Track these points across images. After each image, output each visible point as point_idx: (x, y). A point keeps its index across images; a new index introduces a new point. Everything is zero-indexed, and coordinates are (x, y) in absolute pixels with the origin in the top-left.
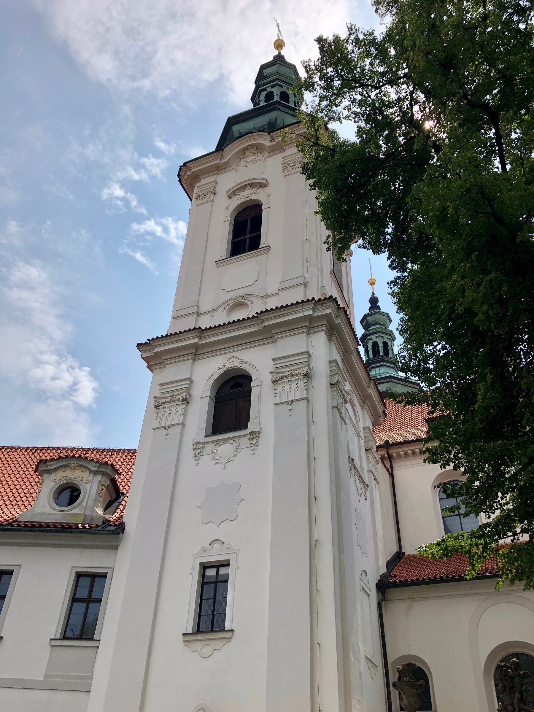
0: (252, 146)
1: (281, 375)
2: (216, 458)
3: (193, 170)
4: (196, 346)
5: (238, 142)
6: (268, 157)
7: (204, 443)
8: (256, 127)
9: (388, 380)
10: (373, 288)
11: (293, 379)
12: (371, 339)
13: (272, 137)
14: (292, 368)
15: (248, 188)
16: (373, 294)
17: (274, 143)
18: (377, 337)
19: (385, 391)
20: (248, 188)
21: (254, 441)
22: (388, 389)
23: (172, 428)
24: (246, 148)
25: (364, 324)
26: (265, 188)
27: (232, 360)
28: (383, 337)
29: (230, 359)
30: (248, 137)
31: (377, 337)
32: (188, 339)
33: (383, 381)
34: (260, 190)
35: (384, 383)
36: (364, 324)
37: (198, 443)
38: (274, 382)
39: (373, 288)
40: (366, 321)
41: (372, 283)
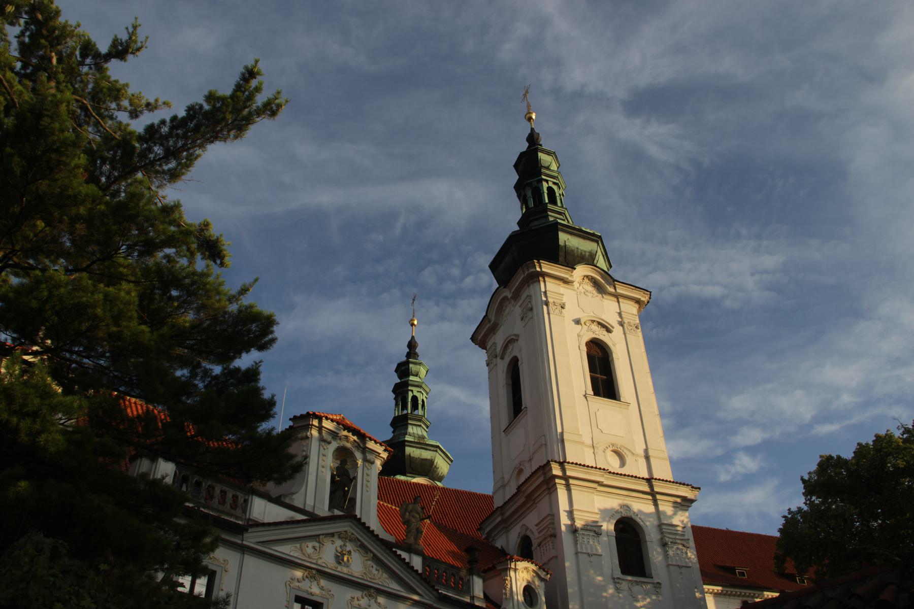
1: (671, 540)
2: (634, 596)
5: (584, 267)
8: (579, 248)
9: (435, 449)
12: (412, 391)
16: (413, 337)
18: (418, 391)
19: (429, 460)
21: (658, 590)
22: (433, 458)
23: (594, 556)
25: (403, 368)
28: (423, 394)
31: (418, 391)
32: (595, 475)
33: (430, 448)
35: (430, 450)
36: (403, 368)
37: (619, 578)
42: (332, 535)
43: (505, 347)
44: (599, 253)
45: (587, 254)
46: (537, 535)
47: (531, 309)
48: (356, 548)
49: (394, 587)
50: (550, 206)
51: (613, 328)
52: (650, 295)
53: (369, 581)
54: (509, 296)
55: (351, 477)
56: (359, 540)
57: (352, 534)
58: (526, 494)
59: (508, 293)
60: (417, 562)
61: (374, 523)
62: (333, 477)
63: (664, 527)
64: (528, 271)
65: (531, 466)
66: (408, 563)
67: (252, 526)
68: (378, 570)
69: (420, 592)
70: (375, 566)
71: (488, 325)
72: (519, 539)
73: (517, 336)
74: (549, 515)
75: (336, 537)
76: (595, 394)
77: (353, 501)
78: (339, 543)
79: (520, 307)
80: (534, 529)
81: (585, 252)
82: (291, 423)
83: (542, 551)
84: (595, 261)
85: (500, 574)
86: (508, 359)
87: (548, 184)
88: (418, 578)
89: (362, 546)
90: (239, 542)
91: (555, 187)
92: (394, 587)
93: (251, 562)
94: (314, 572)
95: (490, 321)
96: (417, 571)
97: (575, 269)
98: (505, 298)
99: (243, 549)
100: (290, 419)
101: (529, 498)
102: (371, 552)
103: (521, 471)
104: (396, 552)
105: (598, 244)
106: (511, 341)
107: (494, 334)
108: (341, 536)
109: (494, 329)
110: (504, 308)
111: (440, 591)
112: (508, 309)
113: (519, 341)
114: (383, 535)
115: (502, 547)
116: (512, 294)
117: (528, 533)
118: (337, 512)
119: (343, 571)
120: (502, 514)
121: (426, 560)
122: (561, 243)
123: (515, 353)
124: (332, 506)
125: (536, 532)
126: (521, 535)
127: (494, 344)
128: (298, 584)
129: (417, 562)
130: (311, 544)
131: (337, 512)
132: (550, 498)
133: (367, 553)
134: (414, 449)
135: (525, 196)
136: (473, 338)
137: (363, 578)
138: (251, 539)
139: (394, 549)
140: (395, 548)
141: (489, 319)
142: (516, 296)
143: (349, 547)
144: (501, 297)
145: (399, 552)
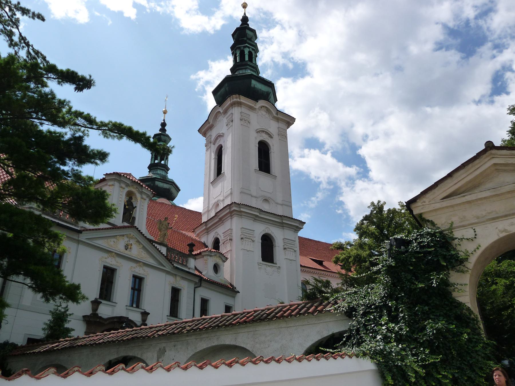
0: (266, 107)
1: (287, 247)
3: (241, 100)
4: (257, 216)
6: (271, 119)
7: (262, 264)
8: (262, 89)
10: (164, 116)
11: (291, 250)
13: (277, 113)
14: (291, 246)
15: (265, 132)
17: (276, 116)
20: (265, 132)
21: (279, 270)
24: (264, 106)
26: (271, 139)
27: (268, 229)
29: (267, 228)
30: (267, 102)
34: (269, 138)
37: (260, 263)
38: (285, 249)
39: (164, 116)
40: (159, 137)
41: (165, 112)
42: (123, 235)
43: (216, 139)
44: (272, 94)
45: (265, 93)
46: (223, 238)
47: (232, 121)
48: (134, 242)
49: (152, 262)
50: (249, 63)
51: (274, 136)
52: (295, 120)
53: (140, 259)
54: (221, 112)
55: (134, 206)
56: (136, 238)
57: (133, 235)
58: (219, 217)
59: (221, 110)
60: (164, 250)
61: (144, 230)
62: (125, 206)
63: (285, 240)
64: (233, 100)
65: (223, 204)
66: (160, 251)
67: (84, 230)
68: (145, 254)
69: (164, 265)
70: (143, 251)
71: (208, 125)
72: (213, 239)
73: (224, 134)
74: (230, 229)
75: (125, 236)
76: (259, 170)
77: (134, 218)
78: (126, 239)
79: (226, 118)
80: (222, 235)
81: (264, 92)
82: (104, 177)
83: (225, 247)
84: (269, 98)
85: (203, 257)
86: (217, 145)
87: (249, 49)
88: (165, 258)
89: (138, 241)
90: (77, 238)
91: (253, 52)
92: (152, 262)
93: (81, 247)
94: (114, 254)
95: (209, 123)
96: (164, 255)
97: (258, 102)
98: (220, 112)
99: (79, 242)
100: (104, 175)
101: (221, 219)
102: (142, 244)
103: (217, 205)
104: (154, 245)
105: (272, 89)
106: (220, 136)
107: (211, 130)
108: (127, 236)
109: (211, 127)
110: (218, 117)
111: (174, 265)
112: (220, 118)
113: (224, 137)
114: (149, 236)
115: (204, 242)
116: (223, 111)
117: (218, 237)
118: (126, 224)
119: (127, 253)
120: (206, 225)
121: (169, 250)
122: (252, 86)
123: (221, 143)
124: (123, 221)
125: (222, 237)
126: (214, 237)
127: (211, 135)
128: (105, 260)
129: (164, 250)
130: (112, 240)
131: (126, 224)
132: (231, 221)
133: (140, 245)
134: (160, 183)
135: (236, 54)
136: (199, 131)
137: (137, 257)
138: (83, 237)
139: (154, 244)
140: (154, 243)
141: (209, 122)
142: (225, 112)
143: (132, 242)
144: (216, 112)
145: (156, 245)
